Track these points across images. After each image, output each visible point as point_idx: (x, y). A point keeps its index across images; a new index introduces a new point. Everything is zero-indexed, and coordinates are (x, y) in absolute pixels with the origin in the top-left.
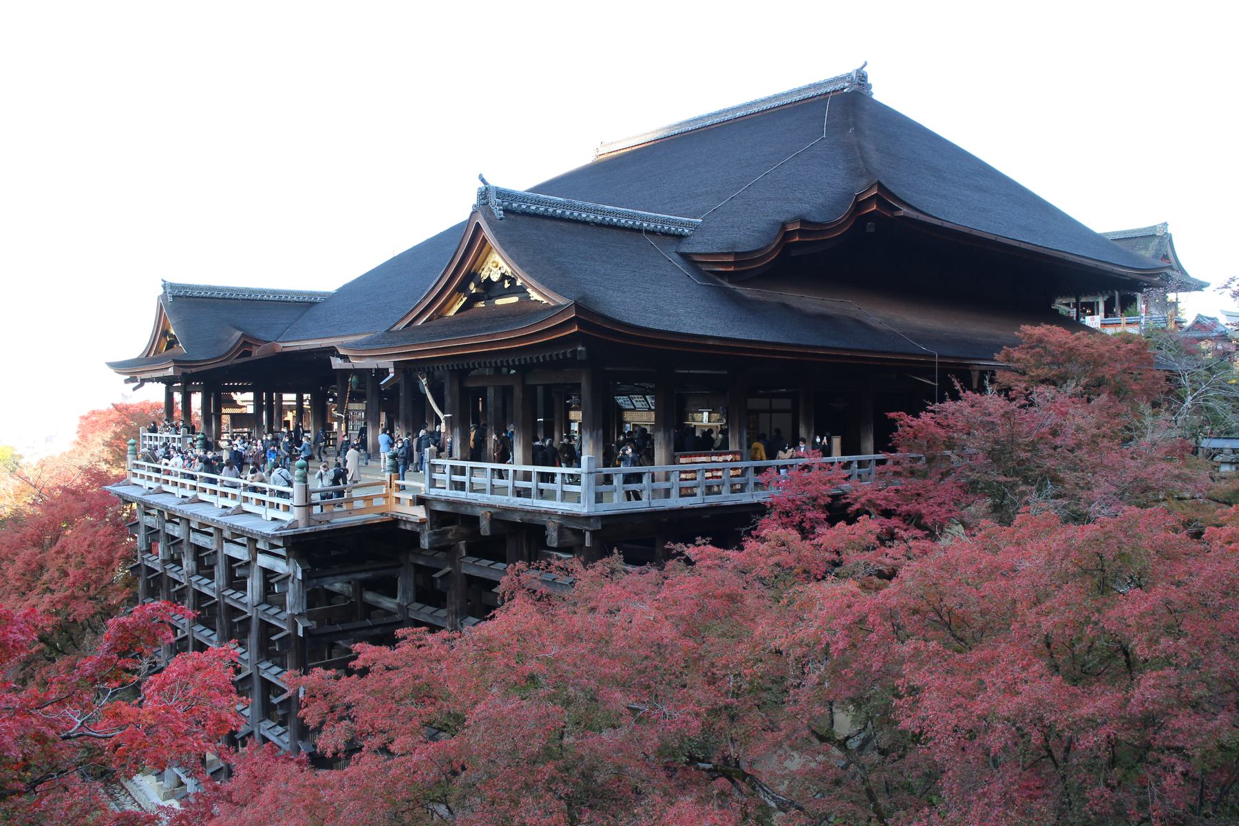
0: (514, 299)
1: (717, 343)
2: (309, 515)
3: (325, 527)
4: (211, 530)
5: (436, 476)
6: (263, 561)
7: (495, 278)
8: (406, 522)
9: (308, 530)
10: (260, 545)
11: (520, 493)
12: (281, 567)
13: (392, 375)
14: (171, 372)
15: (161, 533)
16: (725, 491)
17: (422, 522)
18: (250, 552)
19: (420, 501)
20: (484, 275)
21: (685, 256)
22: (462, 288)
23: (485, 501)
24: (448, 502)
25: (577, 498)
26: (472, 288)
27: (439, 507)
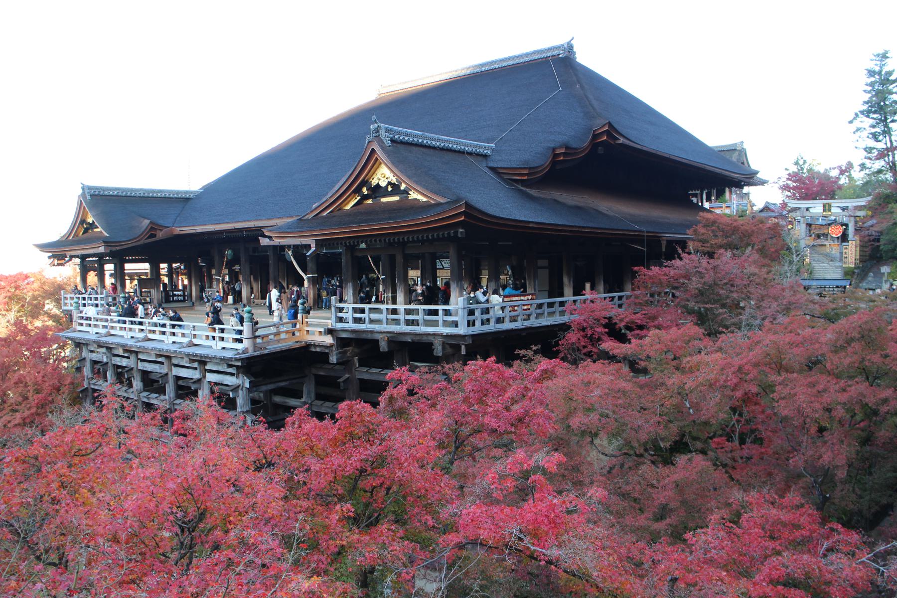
0: (396, 198)
1: (535, 226)
2: (255, 344)
3: (266, 352)
4: (160, 359)
6: (210, 377)
7: (383, 184)
8: (315, 346)
9: (256, 354)
10: (208, 367)
13: (313, 249)
14: (102, 249)
15: (110, 364)
16: (533, 318)
18: (201, 372)
19: (330, 332)
20: (374, 182)
21: (493, 169)
23: (382, 329)
25: (456, 324)
26: (365, 191)
27: (344, 335)
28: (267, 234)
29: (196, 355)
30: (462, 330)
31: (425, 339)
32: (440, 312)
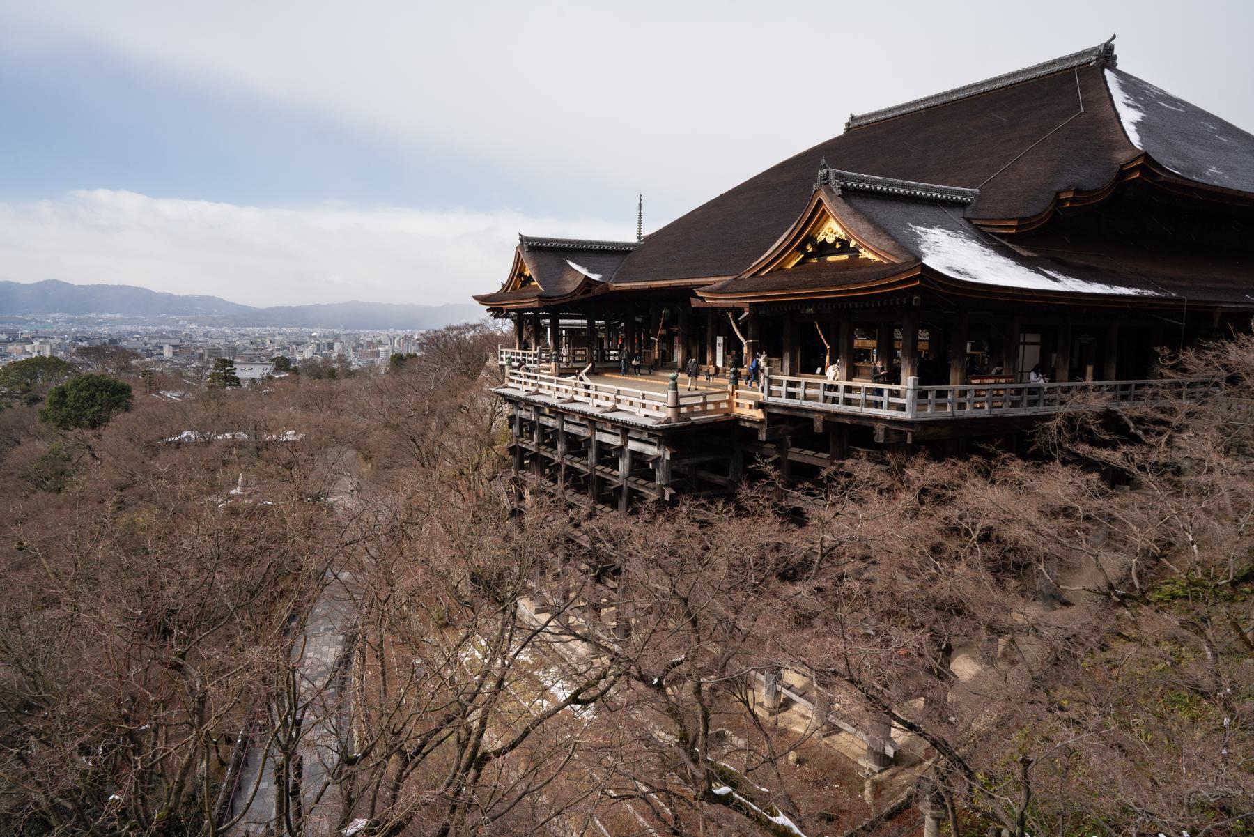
2: (678, 414)
5: (773, 388)
6: (632, 445)
7: (830, 240)
8: (744, 421)
11: (848, 402)
12: (651, 450)
14: (535, 305)
17: (762, 421)
19: (760, 405)
20: (820, 238)
22: (801, 248)
23: (818, 407)
24: (786, 408)
25: (902, 408)
26: (809, 248)
27: (776, 411)
28: (699, 294)
29: (616, 421)
30: (907, 415)
31: (865, 423)
32: (886, 393)
